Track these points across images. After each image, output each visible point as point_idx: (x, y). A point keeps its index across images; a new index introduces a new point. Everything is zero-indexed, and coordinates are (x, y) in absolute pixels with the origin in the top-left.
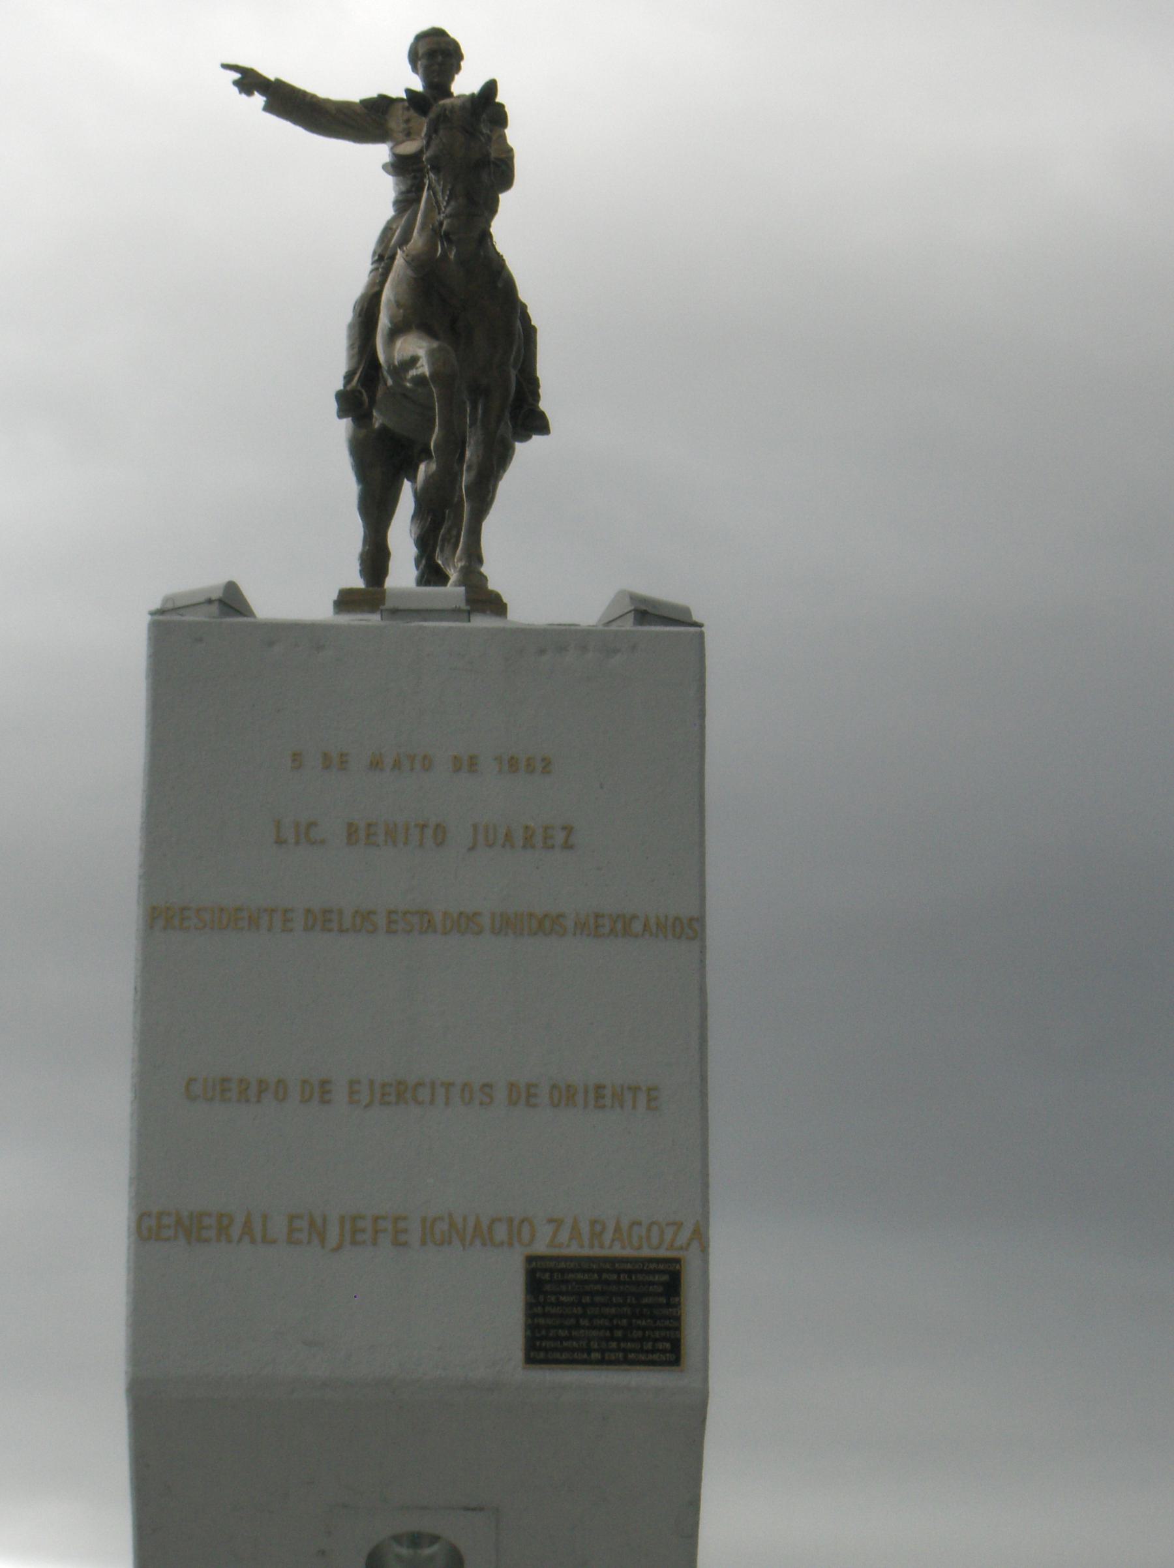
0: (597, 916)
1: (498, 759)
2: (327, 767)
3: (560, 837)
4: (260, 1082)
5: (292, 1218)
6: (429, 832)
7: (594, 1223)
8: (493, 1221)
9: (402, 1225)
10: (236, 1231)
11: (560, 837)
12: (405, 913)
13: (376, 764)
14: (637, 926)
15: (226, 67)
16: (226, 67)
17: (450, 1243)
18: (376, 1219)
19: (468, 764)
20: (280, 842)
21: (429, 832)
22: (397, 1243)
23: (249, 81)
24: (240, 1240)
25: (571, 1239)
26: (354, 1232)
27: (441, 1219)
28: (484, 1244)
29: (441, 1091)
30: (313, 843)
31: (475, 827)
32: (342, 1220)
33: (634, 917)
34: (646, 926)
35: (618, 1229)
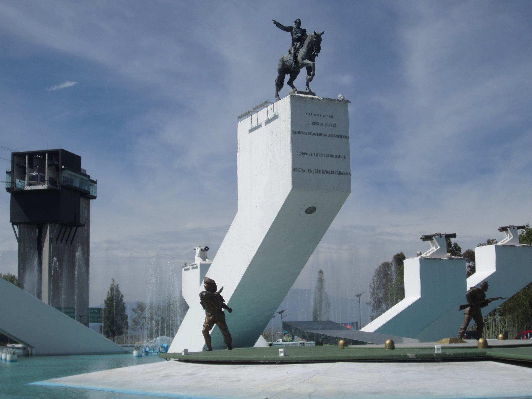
1: (328, 115)
2: (310, 115)
5: (309, 169)
6: (321, 124)
7: (339, 172)
10: (303, 170)
11: (334, 125)
13: (315, 115)
14: (343, 137)
15: (273, 20)
16: (273, 20)
21: (321, 124)
23: (275, 22)
26: (315, 171)
30: (309, 124)
32: (314, 170)
33: (342, 136)
34: (344, 137)
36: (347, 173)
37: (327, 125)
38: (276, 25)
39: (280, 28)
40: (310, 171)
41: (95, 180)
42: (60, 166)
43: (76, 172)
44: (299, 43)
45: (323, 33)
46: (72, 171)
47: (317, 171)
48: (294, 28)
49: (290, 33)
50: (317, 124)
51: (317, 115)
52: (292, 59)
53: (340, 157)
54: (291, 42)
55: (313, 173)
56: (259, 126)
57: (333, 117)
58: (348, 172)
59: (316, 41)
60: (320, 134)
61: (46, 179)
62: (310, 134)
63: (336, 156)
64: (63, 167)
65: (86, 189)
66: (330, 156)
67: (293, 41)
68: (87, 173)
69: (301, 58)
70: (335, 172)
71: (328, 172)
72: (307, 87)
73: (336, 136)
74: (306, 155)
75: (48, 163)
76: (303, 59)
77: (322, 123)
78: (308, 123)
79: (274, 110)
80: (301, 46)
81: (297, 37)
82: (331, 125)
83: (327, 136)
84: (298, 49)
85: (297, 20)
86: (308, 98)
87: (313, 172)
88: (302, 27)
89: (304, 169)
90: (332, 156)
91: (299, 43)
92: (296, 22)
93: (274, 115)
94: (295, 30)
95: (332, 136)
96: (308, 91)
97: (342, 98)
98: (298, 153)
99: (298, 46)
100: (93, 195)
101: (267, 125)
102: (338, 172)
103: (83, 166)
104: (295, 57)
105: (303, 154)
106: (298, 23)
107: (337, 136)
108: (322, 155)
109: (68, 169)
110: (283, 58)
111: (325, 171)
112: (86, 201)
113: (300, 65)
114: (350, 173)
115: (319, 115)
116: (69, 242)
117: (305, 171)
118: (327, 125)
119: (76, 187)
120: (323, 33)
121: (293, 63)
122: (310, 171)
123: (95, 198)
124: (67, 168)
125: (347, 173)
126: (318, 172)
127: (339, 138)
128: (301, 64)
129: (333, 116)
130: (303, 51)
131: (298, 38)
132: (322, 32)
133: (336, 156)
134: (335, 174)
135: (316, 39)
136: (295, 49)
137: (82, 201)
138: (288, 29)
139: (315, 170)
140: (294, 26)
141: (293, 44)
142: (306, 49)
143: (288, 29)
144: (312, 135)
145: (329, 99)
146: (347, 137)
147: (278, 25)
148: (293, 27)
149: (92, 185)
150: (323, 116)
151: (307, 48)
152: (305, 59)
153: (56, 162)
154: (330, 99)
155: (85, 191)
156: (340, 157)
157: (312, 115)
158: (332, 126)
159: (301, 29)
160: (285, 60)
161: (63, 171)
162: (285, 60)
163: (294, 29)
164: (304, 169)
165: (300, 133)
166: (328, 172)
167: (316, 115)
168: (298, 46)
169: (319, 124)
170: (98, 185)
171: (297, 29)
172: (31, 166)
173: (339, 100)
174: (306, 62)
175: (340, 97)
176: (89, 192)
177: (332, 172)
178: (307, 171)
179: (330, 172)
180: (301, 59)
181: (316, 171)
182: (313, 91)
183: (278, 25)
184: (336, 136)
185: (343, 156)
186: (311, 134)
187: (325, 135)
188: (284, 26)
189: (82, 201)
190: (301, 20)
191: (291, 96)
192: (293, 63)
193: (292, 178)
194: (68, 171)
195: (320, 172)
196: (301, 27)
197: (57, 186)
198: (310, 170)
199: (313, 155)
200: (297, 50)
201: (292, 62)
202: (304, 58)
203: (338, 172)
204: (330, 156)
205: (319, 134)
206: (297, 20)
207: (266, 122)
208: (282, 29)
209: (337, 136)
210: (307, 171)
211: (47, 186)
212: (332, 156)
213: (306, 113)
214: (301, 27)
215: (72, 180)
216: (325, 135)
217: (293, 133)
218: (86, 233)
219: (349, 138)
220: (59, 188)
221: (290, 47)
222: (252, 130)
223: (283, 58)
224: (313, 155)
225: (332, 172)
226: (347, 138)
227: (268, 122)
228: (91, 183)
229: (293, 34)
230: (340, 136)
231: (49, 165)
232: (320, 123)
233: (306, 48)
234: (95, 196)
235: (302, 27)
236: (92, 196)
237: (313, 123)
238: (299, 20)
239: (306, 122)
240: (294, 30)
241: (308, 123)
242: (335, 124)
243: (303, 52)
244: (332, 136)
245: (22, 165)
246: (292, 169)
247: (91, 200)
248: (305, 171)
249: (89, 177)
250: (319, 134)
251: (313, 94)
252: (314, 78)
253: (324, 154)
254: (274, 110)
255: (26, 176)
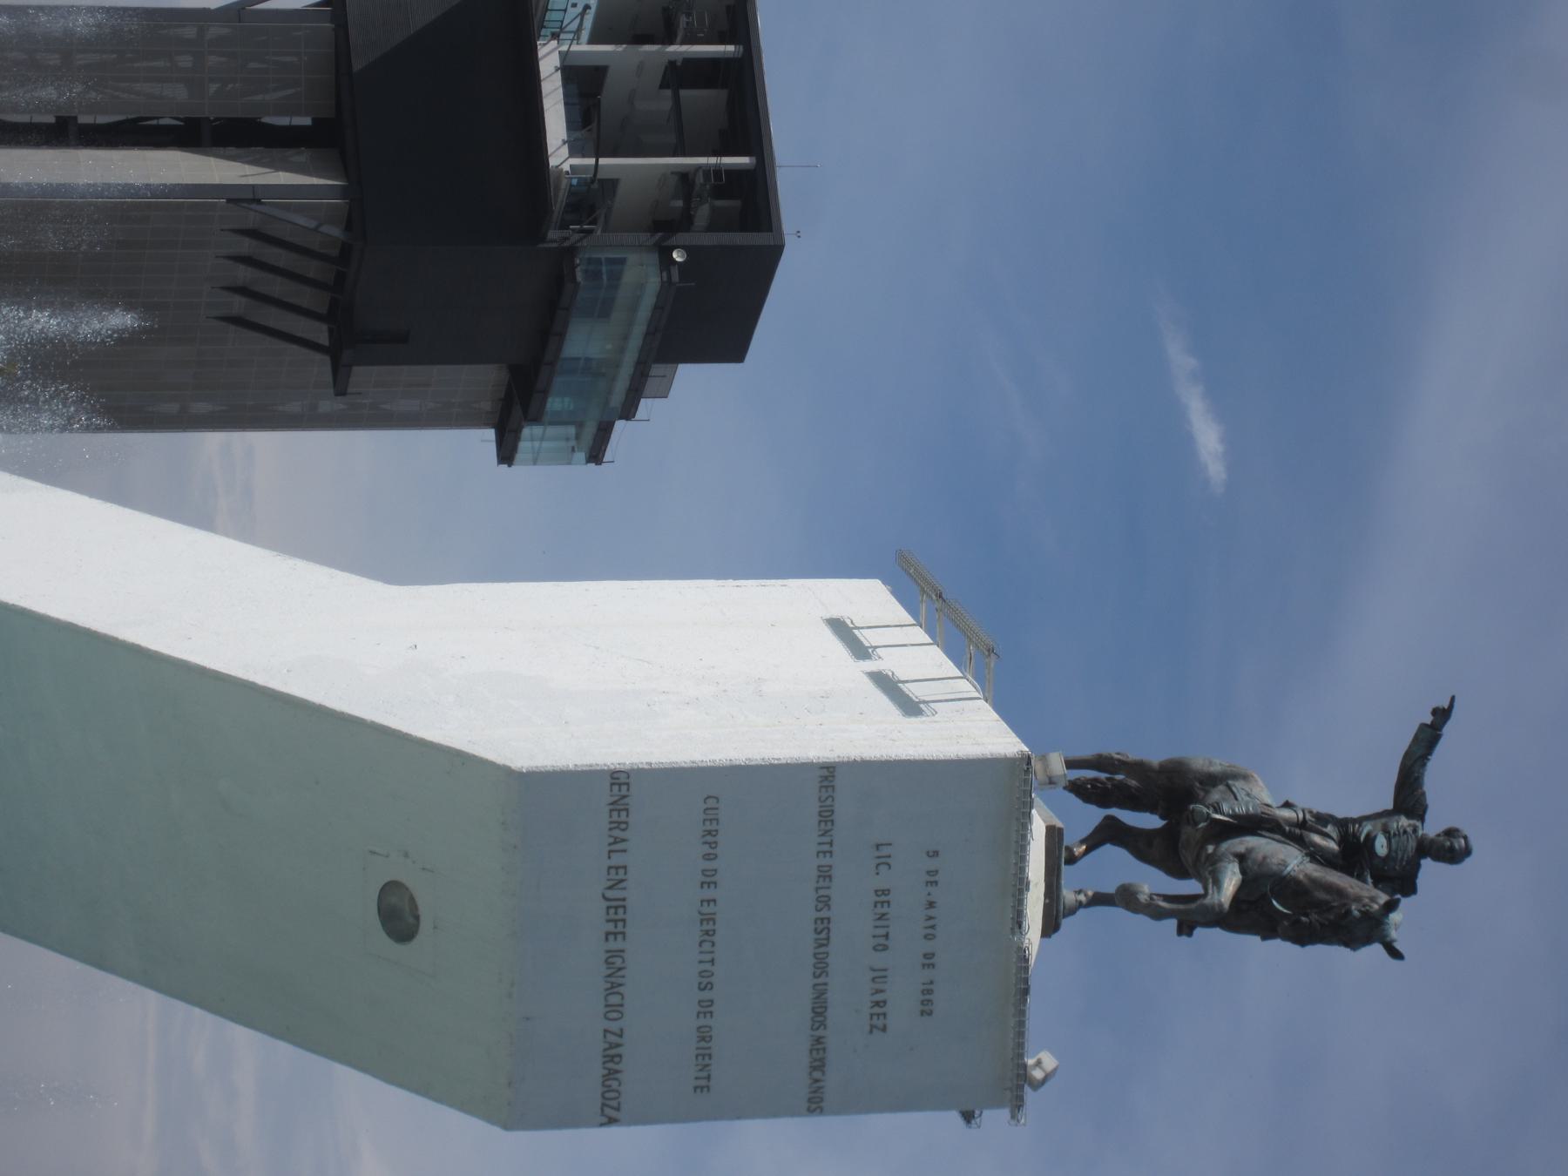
0: (824, 1049)
1: (932, 983)
2: (928, 873)
3: (880, 1023)
4: (716, 843)
6: (882, 941)
7: (620, 1056)
8: (621, 994)
9: (620, 937)
10: (617, 833)
11: (880, 1023)
12: (829, 929)
13: (931, 905)
14: (817, 1075)
15: (1453, 699)
16: (1453, 699)
17: (608, 968)
18: (624, 921)
19: (929, 960)
20: (878, 846)
21: (882, 941)
22: (608, 934)
23: (1442, 715)
24: (605, 1068)
25: (610, 1043)
27: (624, 962)
28: (604, 1076)
29: (708, 957)
31: (885, 970)
32: (624, 900)
33: (823, 1073)
34: (817, 1081)
35: (617, 1072)
36: (614, 1103)
37: (879, 976)
38: (1428, 719)
39: (1410, 747)
40: (617, 877)
41: (608, 456)
42: (682, 238)
43: (649, 334)
44: (1333, 846)
45: (1395, 954)
46: (658, 307)
47: (616, 921)
48: (1418, 824)
49: (1390, 805)
50: (882, 917)
51: (931, 918)
52: (1240, 809)
53: (704, 1058)
54: (1340, 814)
55: (604, 896)
56: (860, 651)
57: (922, 1013)
58: (618, 1109)
59: (1349, 912)
60: (828, 939)
61: (602, 161)
62: (825, 874)
63: (704, 1036)
64: (677, 256)
65: (555, 404)
66: (706, 995)
67: (1342, 823)
68: (645, 406)
69: (1250, 851)
70: (614, 1026)
71: (613, 988)
72: (1090, 893)
73: (820, 1032)
74: (706, 849)
75: (699, 167)
76: (1242, 858)
77: (885, 948)
78: (883, 862)
79: (947, 701)
80: (1316, 855)
81: (1368, 835)
82: (877, 1004)
83: (815, 976)
84: (1300, 841)
85: (1465, 838)
86: (1022, 885)
87: (610, 894)
88: (1429, 869)
89: (624, 840)
90: (706, 1009)
91: (1333, 846)
92: (1451, 833)
93: (925, 702)
94: (1409, 830)
95: (819, 1011)
96: (1068, 896)
97: (1038, 1074)
98: (711, 803)
99: (1317, 839)
100: (524, 445)
101: (866, 680)
102: (618, 1045)
103: (691, 378)
104: (1257, 824)
105: (709, 833)
106: (1448, 843)
107: (819, 1040)
108: (707, 946)
109: (666, 285)
110: (1245, 777)
111: (620, 969)
112: (486, 406)
113: (1210, 849)
114: (612, 1121)
115: (933, 927)
116: (238, 304)
117: (617, 844)
118: (879, 976)
119: (562, 336)
120: (1395, 954)
121: (1218, 810)
122: (617, 877)
123: (506, 455)
124: (676, 277)
125: (614, 1103)
126: (610, 927)
127: (811, 1051)
128: (1215, 850)
129: (930, 1013)
130: (1292, 861)
131: (1362, 839)
132: (1397, 945)
133: (704, 1036)
134: (606, 1031)
135: (1356, 913)
136: (1303, 825)
137: (484, 379)
138: (1409, 796)
139: (624, 907)
140: (1432, 827)
141: (1323, 819)
142: (1301, 877)
143: (1409, 796)
144: (817, 889)
145: (1026, 981)
146: (815, 1104)
147: (1428, 738)
148: (1422, 818)
149: (577, 437)
150: (926, 956)
151: (1305, 881)
152: (1243, 871)
153: (702, 213)
154: (1026, 992)
155: (545, 393)
156: (704, 1058)
157: (930, 889)
158: (877, 1010)
159: (1415, 868)
160: (1238, 785)
161: (653, 258)
162: (1238, 785)
163: (1412, 822)
164: (624, 840)
165: (826, 817)
166: (613, 988)
167: (931, 912)
168: (1317, 839)
169: (882, 931)
170: (583, 471)
171: (1412, 844)
172: (681, 75)
173: (1021, 1056)
174: (1229, 873)
175: (1039, 1063)
176: (536, 419)
177: (614, 1010)
178: (617, 860)
179: (614, 999)
180: (1241, 849)
181: (616, 910)
182: (1067, 924)
183: (1428, 738)
184: (820, 1032)
185: (709, 1078)
186: (821, 884)
187: (821, 966)
188: (1424, 765)
189: (484, 379)
190: (1468, 861)
191: (1029, 758)
192: (1218, 810)
193: (571, 767)
194: (653, 283)
195: (611, 938)
196: (1427, 865)
197: (564, 226)
198: (621, 875)
199: (709, 893)
200: (1296, 834)
201: (1225, 808)
202: (1249, 862)
203: (618, 1045)
204: (706, 995)
205: (823, 928)
206: (1463, 841)
207: (887, 675)
208: (1408, 755)
209: (819, 1040)
210: (617, 860)
211: (566, 167)
212: (706, 1009)
213: (936, 854)
214: (1427, 865)
215: (603, 310)
216: (821, 966)
217: (825, 773)
218: (294, 407)
219: (811, 1111)
220: (553, 234)
221: (1306, 806)
222: (840, 628)
223: (1245, 777)
224: (709, 893)
225: (614, 1010)
226: (810, 1100)
227: (886, 683)
228: (590, 430)
229: (1383, 820)
230: (822, 1060)
231: (685, 178)
232: (887, 936)
233: (1306, 875)
234: (519, 456)
235: (1429, 869)
236: (517, 438)
237: (886, 892)
238: (1467, 852)
239: (885, 851)
240: (1404, 821)
241: (883, 862)
242: (884, 1029)
243: (1281, 856)
244: (819, 1011)
245: (683, 20)
246: (622, 768)
247: (490, 434)
248: (617, 844)
249: (628, 412)
250: (823, 928)
251: (1051, 926)
252: (1142, 919)
253: (712, 961)
254: (947, 701)
255: (621, 48)
